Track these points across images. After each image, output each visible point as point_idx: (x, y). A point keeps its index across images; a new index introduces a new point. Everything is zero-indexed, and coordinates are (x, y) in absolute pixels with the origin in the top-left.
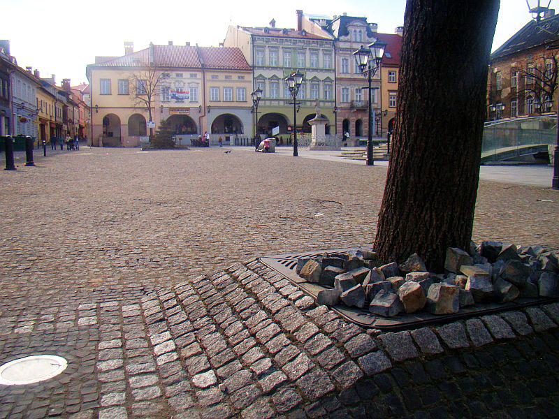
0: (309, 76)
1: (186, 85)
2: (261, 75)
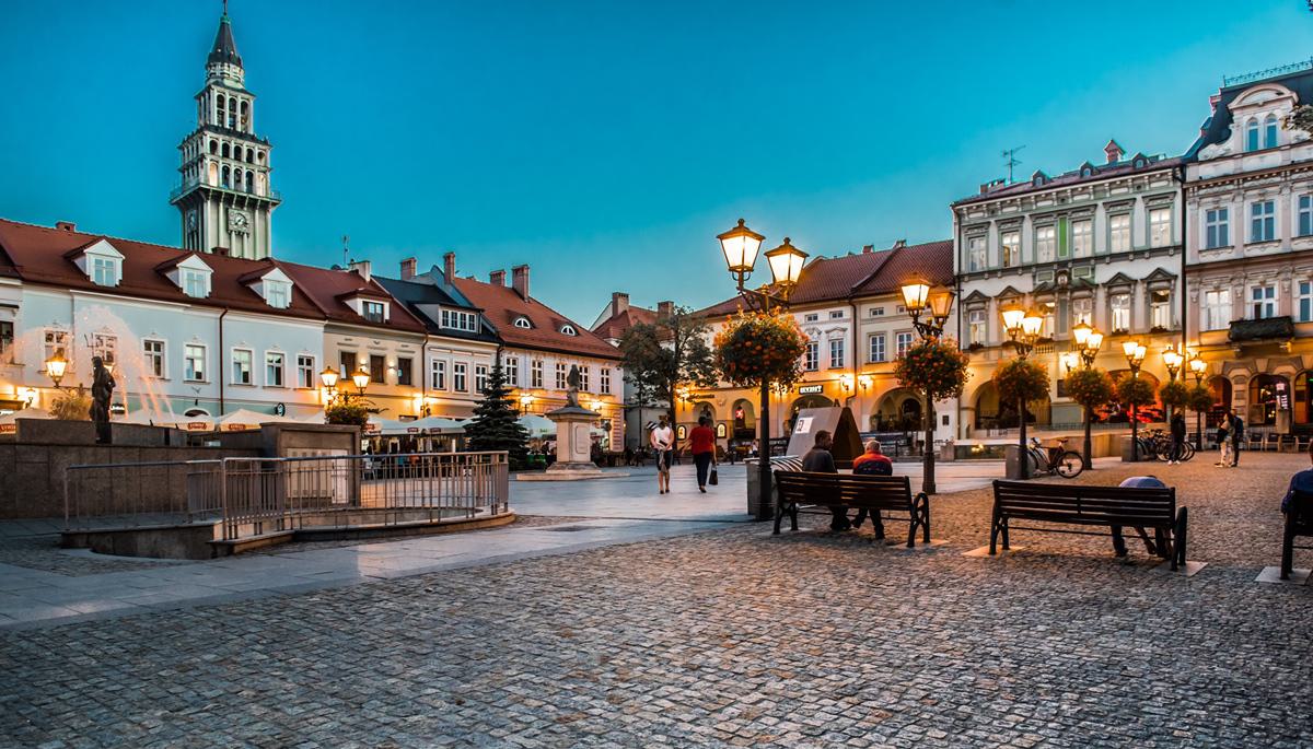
0: (1104, 274)
1: (824, 335)
2: (976, 293)
